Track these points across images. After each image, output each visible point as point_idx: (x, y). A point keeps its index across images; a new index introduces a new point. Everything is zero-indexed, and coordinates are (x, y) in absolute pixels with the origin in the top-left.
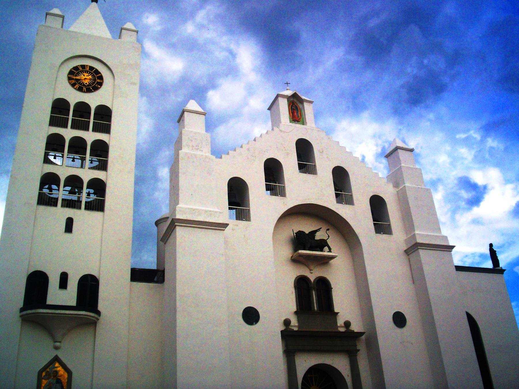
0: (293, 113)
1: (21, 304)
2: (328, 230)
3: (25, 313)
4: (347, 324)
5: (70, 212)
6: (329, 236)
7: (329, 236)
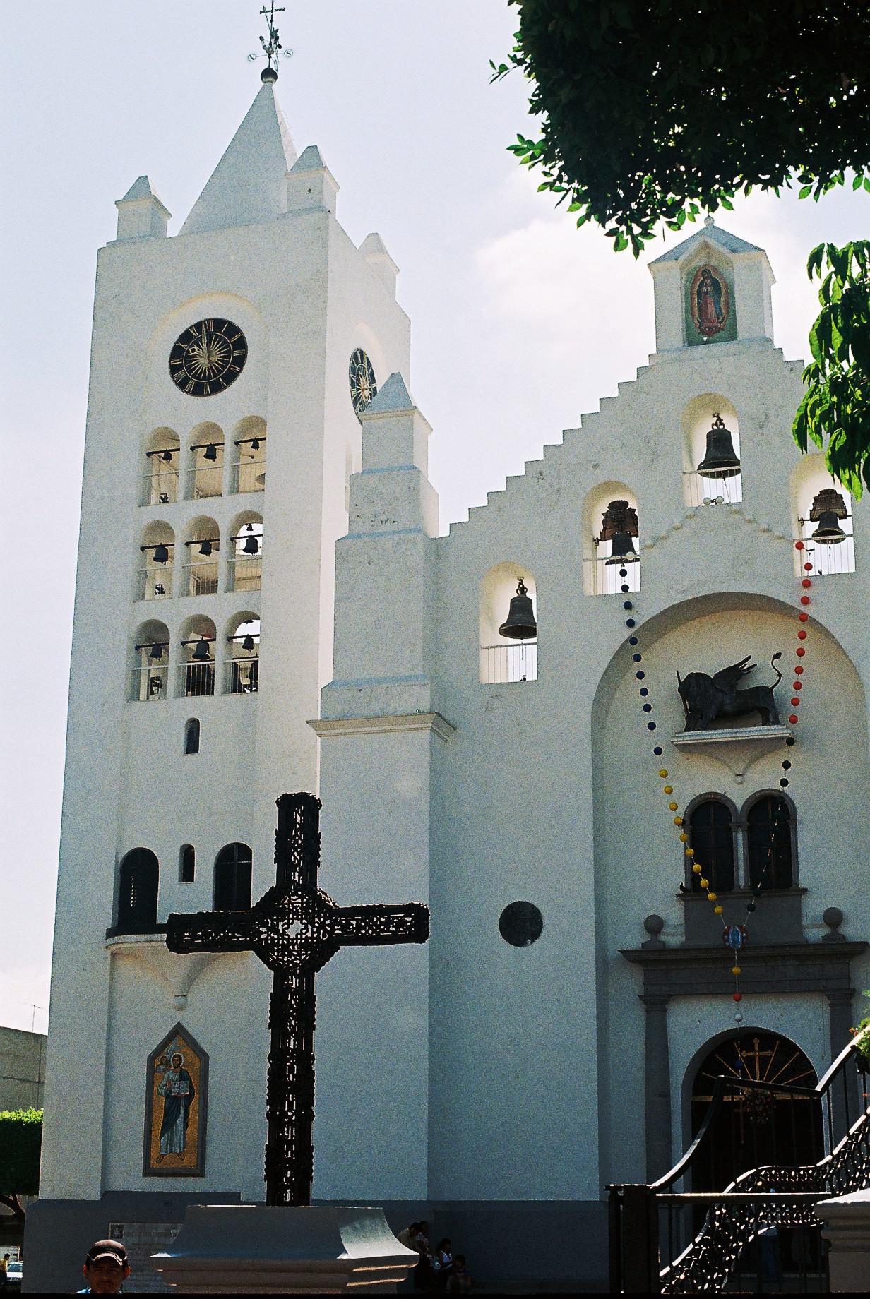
0: (702, 309)
1: (108, 924)
2: (778, 656)
3: (110, 941)
4: (834, 918)
5: (196, 706)
6: (780, 675)
7: (780, 675)
